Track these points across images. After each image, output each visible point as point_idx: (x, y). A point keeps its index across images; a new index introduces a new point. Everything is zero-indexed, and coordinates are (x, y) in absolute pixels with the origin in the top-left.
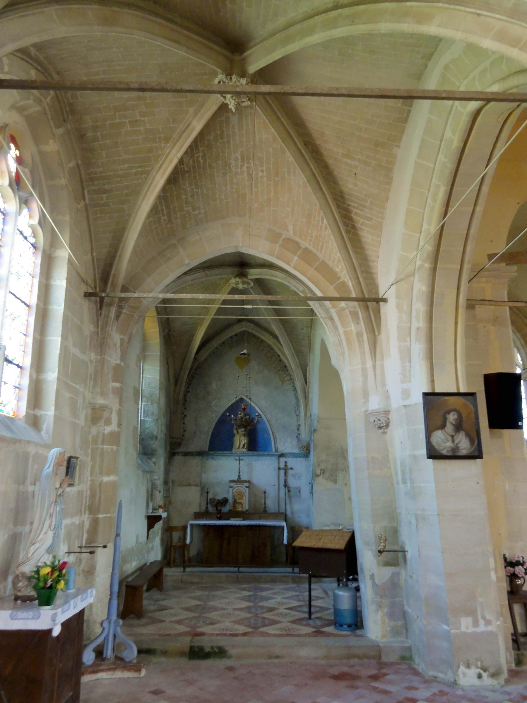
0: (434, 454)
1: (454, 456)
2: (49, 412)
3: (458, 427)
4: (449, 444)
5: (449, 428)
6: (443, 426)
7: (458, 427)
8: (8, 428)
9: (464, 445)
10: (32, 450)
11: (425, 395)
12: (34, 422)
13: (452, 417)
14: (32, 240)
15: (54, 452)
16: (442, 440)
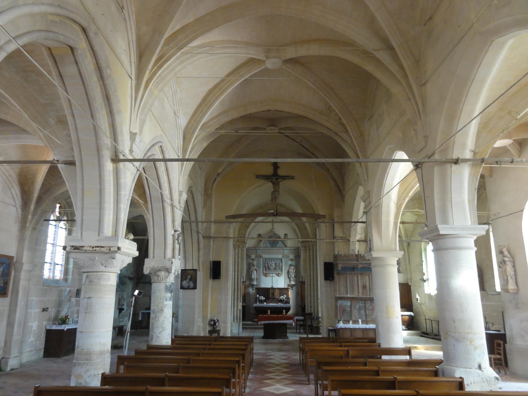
0: (182, 288)
1: (188, 288)
2: (70, 277)
3: (190, 280)
4: (187, 285)
5: (188, 280)
6: (186, 279)
7: (190, 280)
8: (57, 283)
9: (192, 285)
10: (64, 288)
11: (182, 270)
12: (66, 280)
13: (189, 277)
14: (65, 227)
15: (68, 289)
16: (184, 283)
